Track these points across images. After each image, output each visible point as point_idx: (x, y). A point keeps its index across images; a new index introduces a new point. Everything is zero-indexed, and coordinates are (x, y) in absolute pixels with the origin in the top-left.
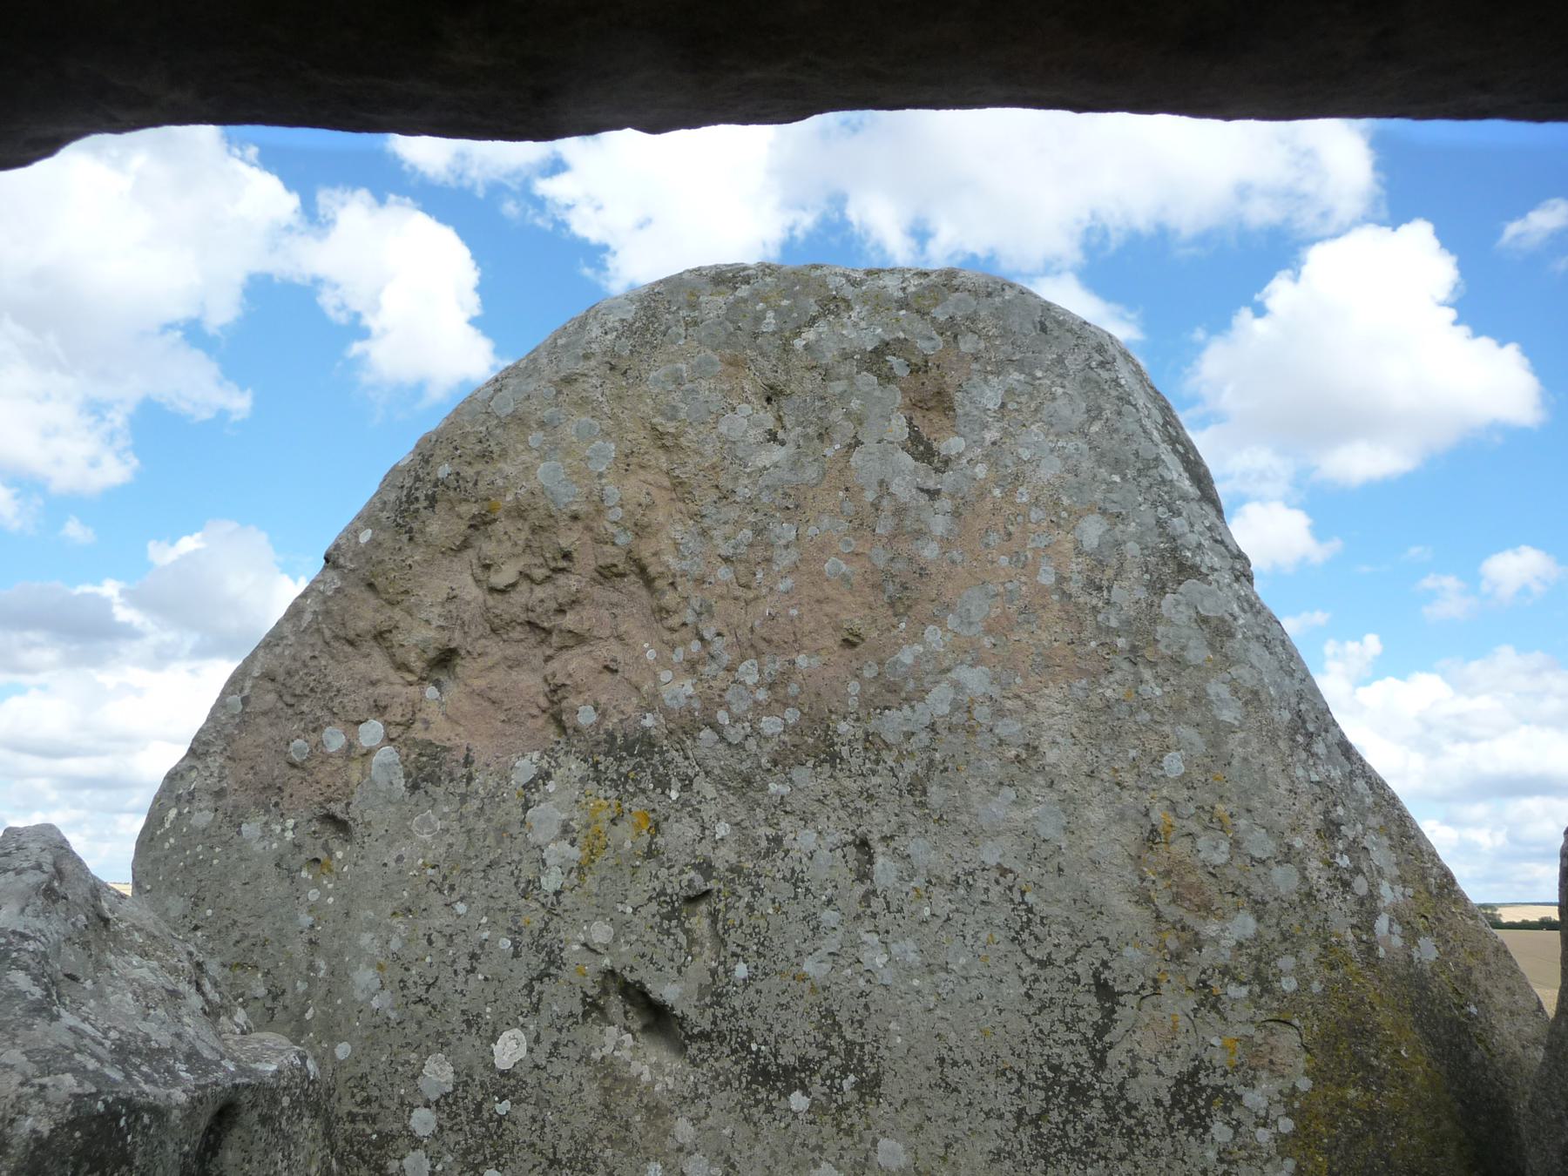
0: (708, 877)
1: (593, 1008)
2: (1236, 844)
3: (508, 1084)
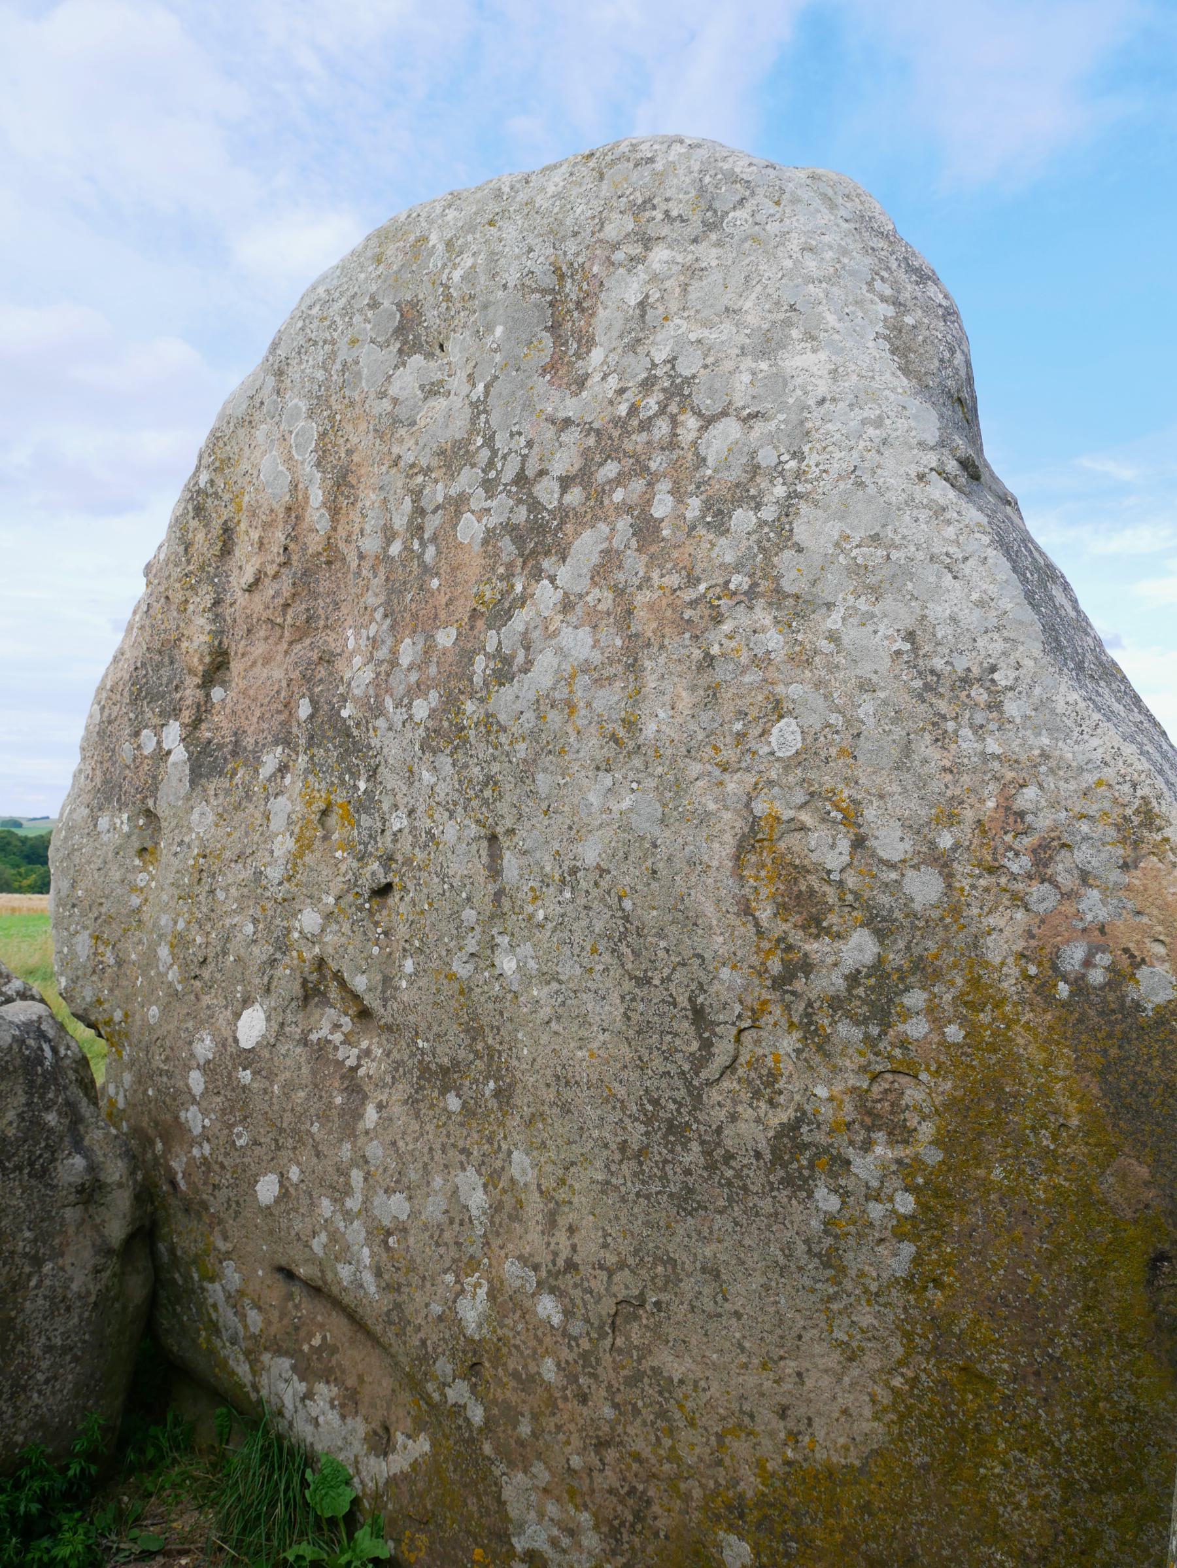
0: (387, 869)
2: (859, 843)
3: (247, 1058)
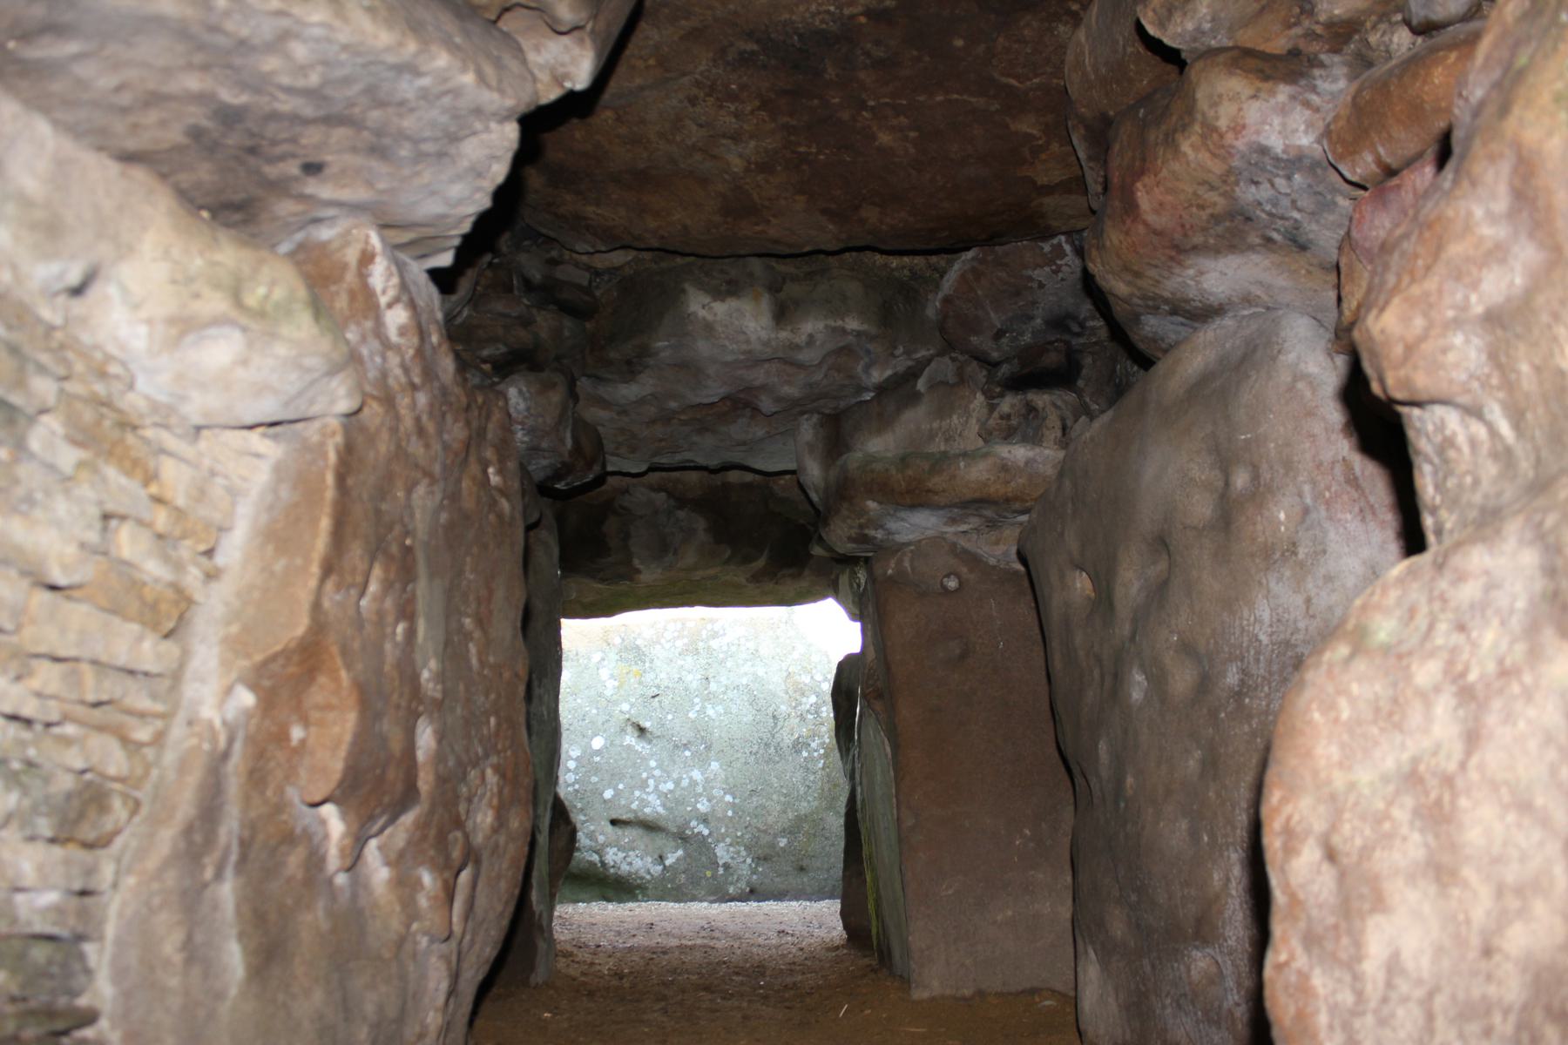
1: (623, 730)
